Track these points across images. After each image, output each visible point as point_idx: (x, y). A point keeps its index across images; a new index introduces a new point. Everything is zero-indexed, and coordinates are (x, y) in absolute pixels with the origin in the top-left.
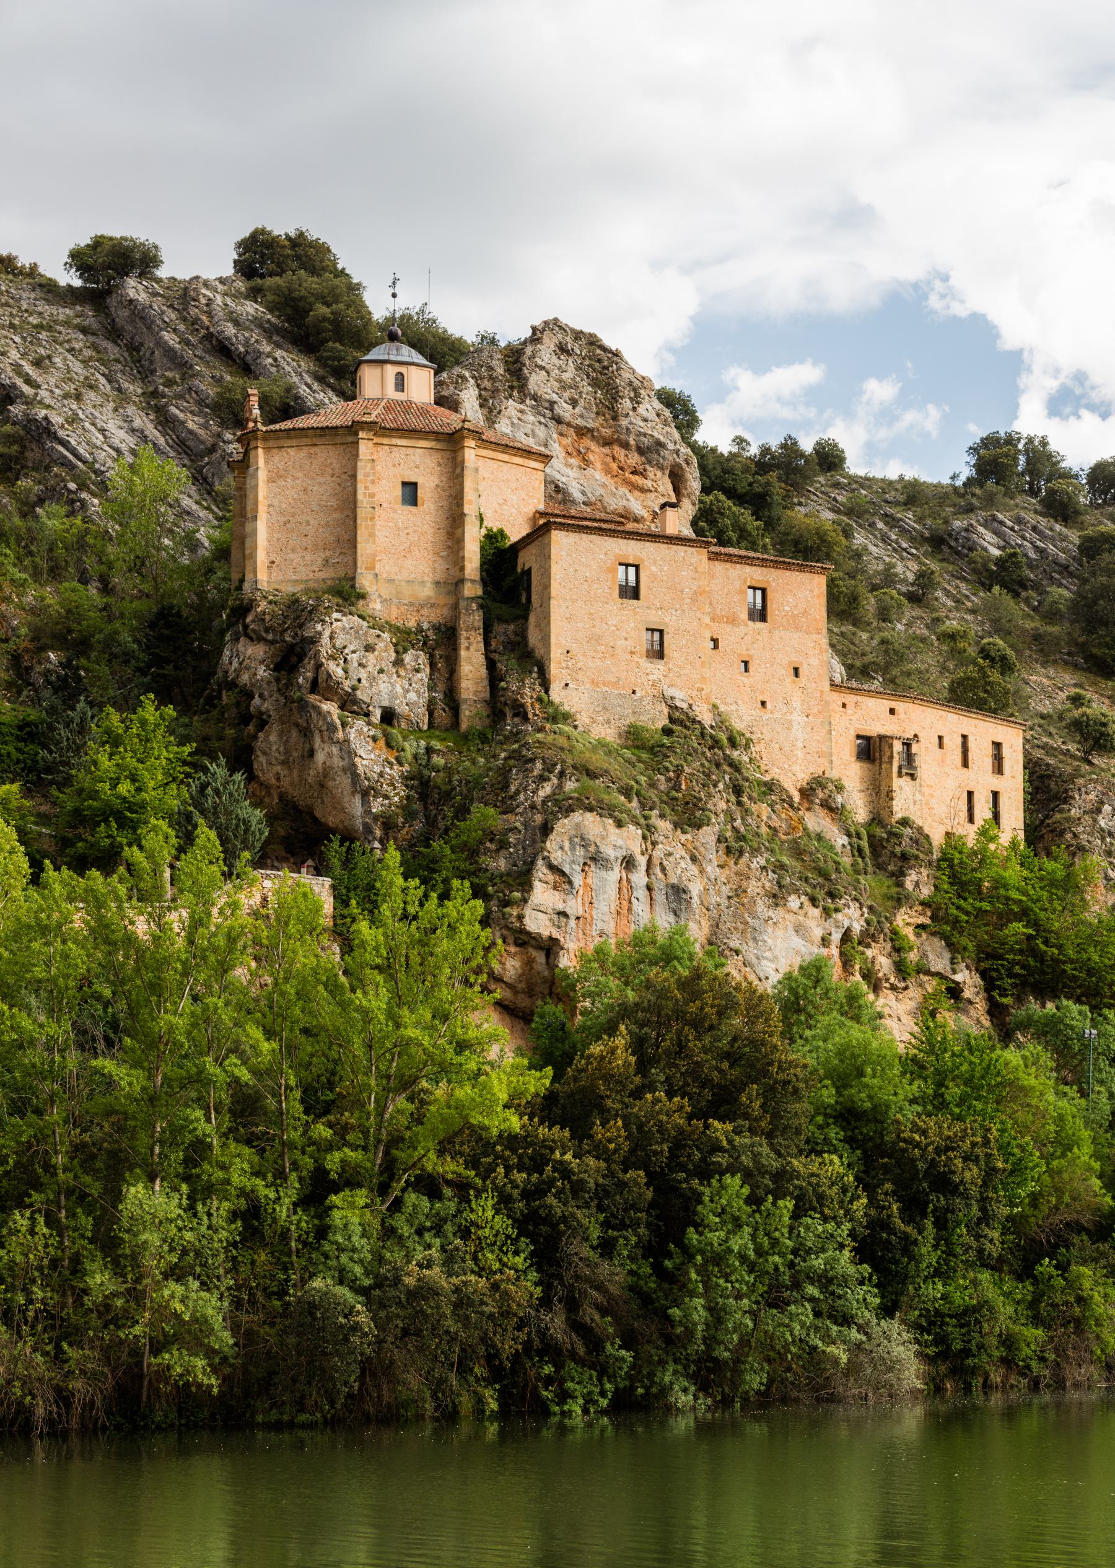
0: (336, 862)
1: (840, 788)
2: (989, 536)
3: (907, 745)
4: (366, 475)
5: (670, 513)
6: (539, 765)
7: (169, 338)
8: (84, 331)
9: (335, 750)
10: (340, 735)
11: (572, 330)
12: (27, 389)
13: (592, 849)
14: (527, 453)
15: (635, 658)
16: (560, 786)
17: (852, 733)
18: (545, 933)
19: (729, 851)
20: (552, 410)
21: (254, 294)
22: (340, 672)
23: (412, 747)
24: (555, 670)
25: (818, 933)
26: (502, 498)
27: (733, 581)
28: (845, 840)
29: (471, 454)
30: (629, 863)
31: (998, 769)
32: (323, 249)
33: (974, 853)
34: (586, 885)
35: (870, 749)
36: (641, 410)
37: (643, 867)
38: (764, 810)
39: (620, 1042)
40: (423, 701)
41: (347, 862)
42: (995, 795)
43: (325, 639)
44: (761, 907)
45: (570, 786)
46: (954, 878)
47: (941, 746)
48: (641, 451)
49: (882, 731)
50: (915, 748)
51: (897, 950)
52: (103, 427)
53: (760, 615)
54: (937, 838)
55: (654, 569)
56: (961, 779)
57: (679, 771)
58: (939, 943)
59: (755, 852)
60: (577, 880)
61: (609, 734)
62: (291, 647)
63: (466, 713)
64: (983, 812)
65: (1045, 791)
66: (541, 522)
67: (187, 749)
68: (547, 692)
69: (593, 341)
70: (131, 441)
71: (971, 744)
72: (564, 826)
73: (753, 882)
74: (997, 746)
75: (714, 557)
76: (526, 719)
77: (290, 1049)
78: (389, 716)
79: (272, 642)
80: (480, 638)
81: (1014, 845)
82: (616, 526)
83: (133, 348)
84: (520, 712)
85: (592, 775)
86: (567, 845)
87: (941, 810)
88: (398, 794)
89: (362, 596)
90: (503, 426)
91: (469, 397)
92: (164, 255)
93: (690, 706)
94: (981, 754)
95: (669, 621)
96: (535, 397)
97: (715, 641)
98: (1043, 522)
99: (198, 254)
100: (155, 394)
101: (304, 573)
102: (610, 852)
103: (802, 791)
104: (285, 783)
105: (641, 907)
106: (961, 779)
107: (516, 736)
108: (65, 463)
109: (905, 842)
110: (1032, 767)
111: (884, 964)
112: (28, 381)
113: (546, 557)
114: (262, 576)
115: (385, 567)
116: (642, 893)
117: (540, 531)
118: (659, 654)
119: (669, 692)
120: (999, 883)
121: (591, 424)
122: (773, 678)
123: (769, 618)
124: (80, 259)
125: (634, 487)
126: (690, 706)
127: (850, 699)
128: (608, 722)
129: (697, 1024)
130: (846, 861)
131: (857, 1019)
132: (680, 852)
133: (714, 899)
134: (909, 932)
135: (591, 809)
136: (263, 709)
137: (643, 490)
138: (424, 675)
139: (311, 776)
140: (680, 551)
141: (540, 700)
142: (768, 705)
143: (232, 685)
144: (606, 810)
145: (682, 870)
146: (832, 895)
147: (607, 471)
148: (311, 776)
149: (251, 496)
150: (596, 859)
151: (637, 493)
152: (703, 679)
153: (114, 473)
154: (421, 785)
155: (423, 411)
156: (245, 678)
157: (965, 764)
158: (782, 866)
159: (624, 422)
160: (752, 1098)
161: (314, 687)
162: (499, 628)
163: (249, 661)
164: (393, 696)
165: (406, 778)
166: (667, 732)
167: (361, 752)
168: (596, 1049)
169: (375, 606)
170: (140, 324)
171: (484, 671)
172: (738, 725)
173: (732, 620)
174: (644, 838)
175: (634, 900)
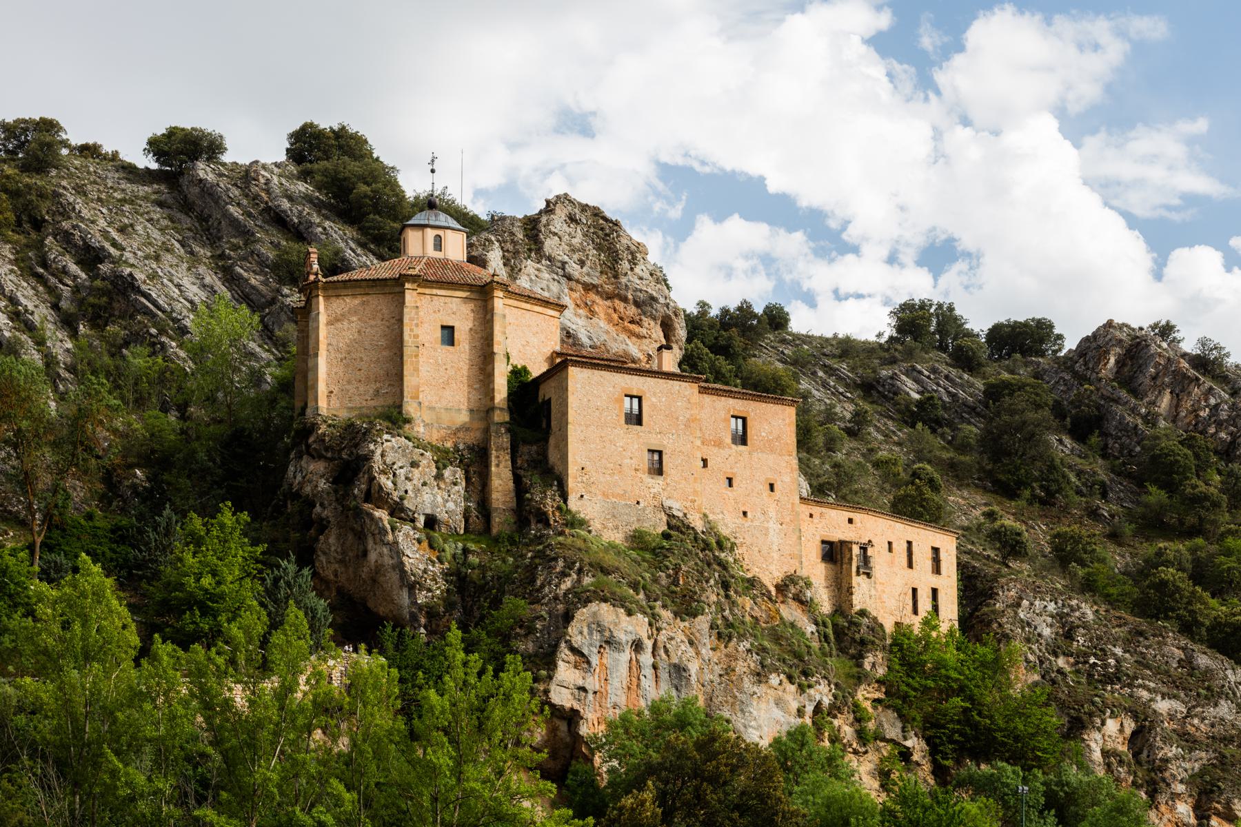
0: (389, 645)
1: (808, 585)
2: (910, 383)
3: (864, 549)
4: (411, 319)
5: (666, 354)
6: (561, 563)
7: (234, 210)
8: (161, 204)
9: (385, 550)
10: (390, 537)
11: (580, 204)
12: (112, 250)
13: (607, 634)
14: (546, 303)
15: (639, 474)
16: (579, 581)
17: (818, 539)
18: (568, 705)
19: (720, 636)
20: (563, 269)
21: (304, 176)
22: (389, 484)
23: (450, 548)
24: (572, 484)
25: (794, 705)
26: (526, 340)
27: (719, 411)
28: (813, 628)
29: (500, 302)
30: (638, 646)
31: (937, 569)
32: (360, 141)
33: (918, 640)
34: (602, 664)
35: (834, 553)
36: (637, 270)
37: (650, 650)
38: (747, 602)
39: (648, 795)
40: (460, 510)
41: (400, 645)
42: (935, 592)
43: (377, 457)
44: (747, 683)
45: (587, 580)
46: (904, 661)
47: (890, 550)
48: (637, 304)
49: (843, 538)
50: (870, 552)
51: (858, 720)
52: (180, 284)
53: (742, 439)
54: (889, 627)
55: (654, 400)
56: (909, 576)
57: (677, 569)
58: (892, 715)
59: (741, 637)
60: (595, 660)
61: (618, 538)
63: (497, 519)
64: (925, 605)
65: (975, 590)
66: (558, 360)
67: (260, 549)
68: (565, 501)
69: (597, 213)
70: (203, 295)
71: (915, 549)
72: (583, 614)
73: (740, 663)
74: (936, 550)
75: (703, 391)
76: (547, 525)
77: (367, 803)
78: (431, 522)
79: (331, 460)
80: (508, 457)
81: (951, 633)
82: (619, 365)
83: (203, 219)
84: (543, 519)
85: (605, 571)
86: (585, 630)
87: (892, 603)
88: (439, 588)
89: (408, 421)
90: (523, 283)
91: (495, 257)
92: (228, 143)
93: (685, 515)
94: (923, 558)
95: (667, 443)
96: (549, 258)
97: (705, 461)
98: (954, 372)
99: (255, 141)
100: (222, 256)
101: (358, 401)
102: (622, 637)
103: (777, 587)
104: (342, 578)
105: (648, 683)
106: (909, 576)
107: (539, 539)
108: (147, 312)
109: (863, 630)
110: (961, 566)
111: (848, 732)
112: (115, 244)
113: (564, 389)
114: (322, 403)
115: (427, 397)
116: (649, 672)
117: (558, 367)
118: (658, 469)
119: (667, 503)
120: (940, 664)
121: (596, 281)
122: (751, 491)
123: (749, 442)
124: (156, 146)
125: (632, 334)
126: (685, 515)
127: (816, 510)
128: (617, 528)
129: (714, 779)
130: (815, 645)
131: (838, 778)
132: (680, 637)
133: (708, 677)
134: (867, 705)
135: (605, 600)
137: (639, 337)
138: (461, 488)
139: (364, 573)
140: (676, 385)
141: (559, 508)
142: (749, 514)
143: (296, 496)
144: (618, 601)
145: (681, 651)
146: (805, 674)
147: (610, 320)
148: (364, 573)
149: (312, 336)
150: (610, 642)
151: (634, 339)
152: (695, 492)
153: (189, 321)
154: (458, 579)
155: (458, 267)
156: (308, 489)
157: (910, 565)
158: (764, 650)
159: (623, 280)
161: (368, 497)
162: (524, 449)
163: (313, 476)
164: (434, 505)
165: (446, 574)
166: (666, 536)
167: (408, 552)
168: (628, 801)
169: (419, 430)
170: (208, 200)
171: (511, 484)
172: (724, 531)
173: (719, 444)
174: (650, 624)
175: (642, 678)
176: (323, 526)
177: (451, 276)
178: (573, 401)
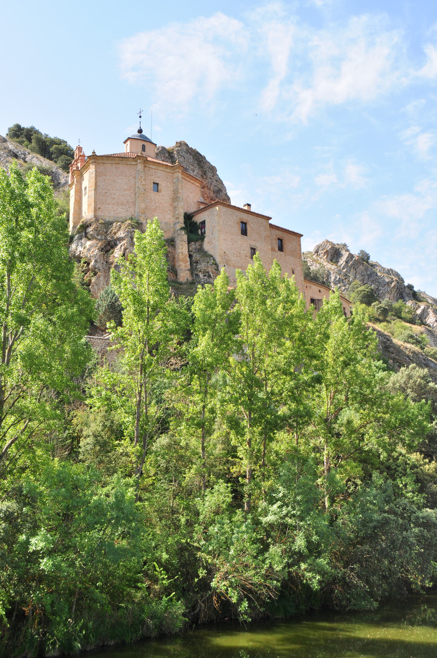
62: (109, 242)
79: (100, 240)
80: (187, 245)
123: (284, 250)
127: (308, 285)
136: (96, 266)
171: (188, 259)
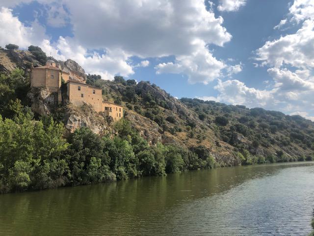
27: (91, 90)
31: (120, 111)
35: (106, 108)
53: (94, 93)
56: (117, 113)
78: (49, 103)
82: (77, 83)
91: (60, 67)
117: (69, 82)
122: (97, 101)
124: (7, 47)
150: (75, 120)
155: (54, 68)
160: (96, 147)
163: (31, 95)
176: (33, 103)
177: (53, 69)
178: (70, 86)
